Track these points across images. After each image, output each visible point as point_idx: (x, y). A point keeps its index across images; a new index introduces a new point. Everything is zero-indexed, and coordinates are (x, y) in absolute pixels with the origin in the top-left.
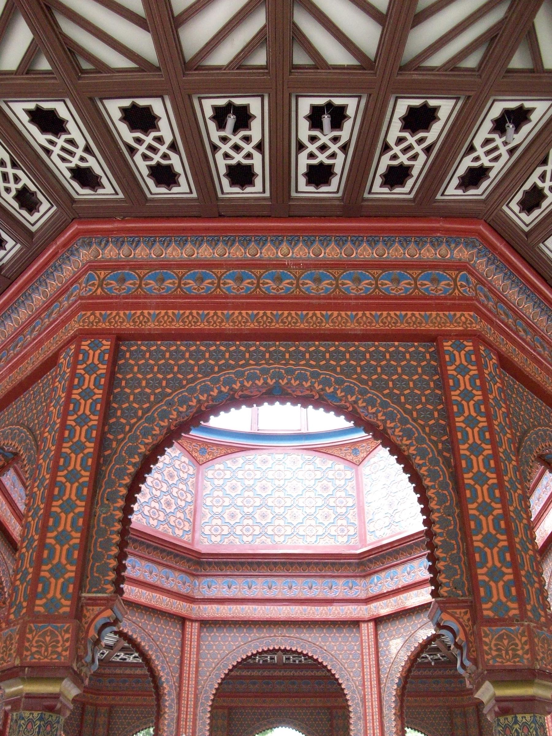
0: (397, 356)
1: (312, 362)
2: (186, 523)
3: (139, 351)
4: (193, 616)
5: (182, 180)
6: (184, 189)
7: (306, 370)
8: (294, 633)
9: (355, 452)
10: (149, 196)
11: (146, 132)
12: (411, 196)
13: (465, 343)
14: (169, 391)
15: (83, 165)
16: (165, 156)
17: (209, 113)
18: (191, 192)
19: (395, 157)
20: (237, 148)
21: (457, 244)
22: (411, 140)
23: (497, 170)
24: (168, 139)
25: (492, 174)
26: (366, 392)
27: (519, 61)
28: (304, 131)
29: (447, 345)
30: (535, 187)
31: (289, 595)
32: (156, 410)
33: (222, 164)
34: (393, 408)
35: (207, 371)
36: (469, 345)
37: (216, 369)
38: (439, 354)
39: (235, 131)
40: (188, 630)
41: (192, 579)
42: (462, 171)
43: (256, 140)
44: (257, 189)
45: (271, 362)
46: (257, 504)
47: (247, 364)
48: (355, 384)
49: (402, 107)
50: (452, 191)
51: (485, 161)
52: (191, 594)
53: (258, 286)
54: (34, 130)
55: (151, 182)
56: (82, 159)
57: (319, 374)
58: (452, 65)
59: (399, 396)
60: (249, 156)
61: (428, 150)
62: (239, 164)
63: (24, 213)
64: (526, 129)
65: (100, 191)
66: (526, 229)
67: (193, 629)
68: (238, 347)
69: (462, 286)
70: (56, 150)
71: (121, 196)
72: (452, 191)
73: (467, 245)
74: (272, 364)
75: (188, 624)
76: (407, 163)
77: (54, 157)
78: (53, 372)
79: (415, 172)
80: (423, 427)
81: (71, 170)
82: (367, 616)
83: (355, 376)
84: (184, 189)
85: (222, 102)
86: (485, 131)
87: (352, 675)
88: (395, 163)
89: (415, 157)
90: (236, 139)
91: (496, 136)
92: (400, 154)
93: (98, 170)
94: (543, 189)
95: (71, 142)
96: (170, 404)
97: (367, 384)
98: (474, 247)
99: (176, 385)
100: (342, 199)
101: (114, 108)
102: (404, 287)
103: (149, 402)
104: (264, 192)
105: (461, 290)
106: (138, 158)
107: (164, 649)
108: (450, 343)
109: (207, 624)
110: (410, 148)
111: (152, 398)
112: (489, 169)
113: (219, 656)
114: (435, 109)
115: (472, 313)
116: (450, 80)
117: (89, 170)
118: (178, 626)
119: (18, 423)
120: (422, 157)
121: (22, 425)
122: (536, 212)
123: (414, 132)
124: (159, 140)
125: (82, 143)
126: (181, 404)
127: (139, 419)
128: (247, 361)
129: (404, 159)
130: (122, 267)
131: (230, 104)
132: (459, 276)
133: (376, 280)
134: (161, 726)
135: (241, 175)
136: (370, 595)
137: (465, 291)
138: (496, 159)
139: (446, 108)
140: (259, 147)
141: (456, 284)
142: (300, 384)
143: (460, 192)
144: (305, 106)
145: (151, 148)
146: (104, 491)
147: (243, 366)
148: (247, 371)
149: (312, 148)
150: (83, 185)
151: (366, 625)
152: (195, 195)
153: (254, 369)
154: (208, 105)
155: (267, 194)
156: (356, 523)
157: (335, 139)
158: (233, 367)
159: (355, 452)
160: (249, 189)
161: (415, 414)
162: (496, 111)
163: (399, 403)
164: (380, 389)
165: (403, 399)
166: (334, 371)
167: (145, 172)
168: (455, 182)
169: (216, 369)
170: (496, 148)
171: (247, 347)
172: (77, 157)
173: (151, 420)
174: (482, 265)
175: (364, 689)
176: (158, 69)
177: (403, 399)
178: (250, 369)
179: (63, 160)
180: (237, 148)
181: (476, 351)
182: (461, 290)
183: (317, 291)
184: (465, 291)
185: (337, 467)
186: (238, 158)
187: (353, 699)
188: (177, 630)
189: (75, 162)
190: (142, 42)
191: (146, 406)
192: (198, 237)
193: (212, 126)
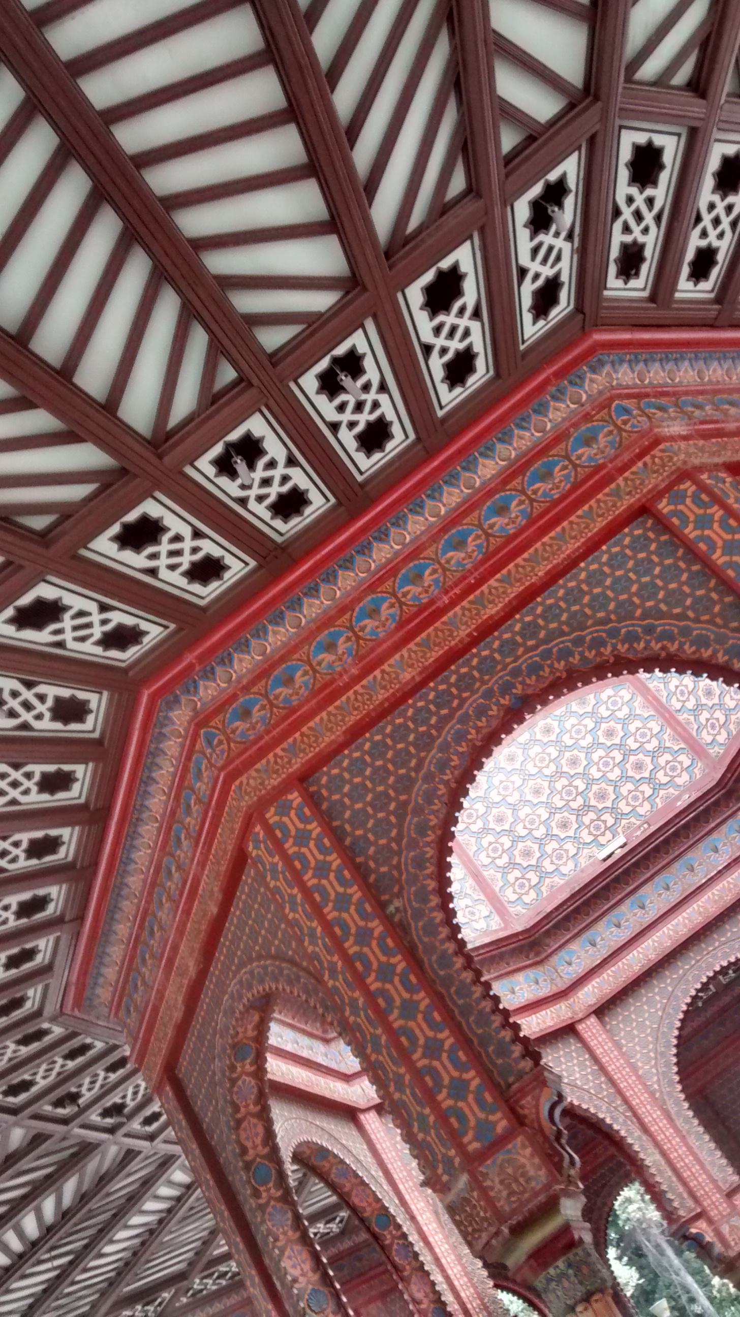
0: (615, 562)
1: (530, 643)
2: (479, 907)
3: (332, 779)
4: (580, 1016)
5: (229, 560)
6: (237, 567)
7: (531, 658)
10: (202, 603)
11: (155, 540)
12: (492, 372)
13: (682, 487)
14: (403, 797)
15: (108, 627)
16: (195, 550)
17: (211, 471)
18: (247, 564)
19: (444, 351)
20: (266, 482)
21: (582, 378)
22: (449, 319)
23: (566, 269)
24: (187, 532)
25: (564, 278)
26: (618, 630)
27: (509, 140)
28: (326, 408)
29: (664, 506)
30: (625, 247)
31: (674, 897)
32: (409, 829)
33: (262, 510)
34: (661, 625)
35: (425, 743)
36: (688, 487)
37: (434, 732)
38: (663, 525)
39: (251, 466)
40: (586, 1035)
41: (540, 968)
42: (527, 300)
43: (281, 458)
44: (319, 502)
45: (486, 677)
47: (463, 701)
48: (597, 631)
49: (415, 294)
50: (531, 329)
51: (547, 272)
52: (555, 990)
53: (401, 604)
54: (29, 634)
55: (197, 588)
56: (104, 622)
57: (549, 651)
58: (441, 208)
59: (656, 606)
60: (285, 479)
61: (476, 314)
62: (281, 497)
63: (74, 726)
64: (569, 202)
65: (146, 640)
66: (646, 294)
67: (591, 1029)
68: (435, 689)
69: (625, 422)
70: (68, 636)
71: (172, 626)
72: (531, 329)
73: (594, 370)
74: (489, 680)
75: (580, 1027)
76: (461, 346)
77: (71, 644)
78: (250, 873)
79: (478, 348)
80: (711, 622)
81: (99, 643)
83: (590, 622)
84: (237, 567)
85: (217, 450)
86: (524, 242)
88: (449, 356)
89: (467, 333)
90: (260, 473)
91: (541, 237)
92: (447, 343)
93: (129, 621)
94: (635, 242)
95: (81, 614)
96: (418, 810)
97: (611, 621)
98: (602, 363)
99: (406, 784)
100: (418, 439)
101: (104, 546)
102: (561, 477)
103: (393, 826)
104: (328, 500)
105: (628, 427)
106: (164, 574)
107: (579, 1082)
108: (665, 501)
109: (602, 1011)
110: (454, 329)
111: (393, 819)
112: (557, 275)
114: (455, 268)
115: (661, 447)
116: (447, 220)
117: (120, 628)
119: (251, 960)
120: (475, 326)
121: (260, 957)
122: (644, 268)
123: (447, 308)
124: (178, 538)
125: (92, 607)
126: (430, 802)
127: (399, 853)
128: (459, 697)
129: (456, 345)
130: (233, 698)
131: (228, 445)
132: (613, 414)
133: (523, 492)
134: (651, 1181)
135: (290, 504)
137: (633, 426)
138: (558, 258)
139: (464, 257)
140: (291, 461)
141: (616, 425)
142: (539, 678)
143: (541, 323)
144: (310, 381)
145: (172, 554)
146: (431, 960)
147: (460, 706)
148: (469, 707)
149: (347, 416)
150: (123, 647)
152: (253, 563)
153: (474, 701)
154: (205, 464)
155: (333, 500)
157: (366, 388)
158: (450, 716)
160: (308, 511)
161: (691, 614)
162: (522, 210)
163: (661, 615)
164: (630, 616)
165: (663, 607)
166: (563, 634)
167: (183, 582)
168: (528, 317)
169: (434, 732)
170: (551, 249)
171: (446, 681)
172: (96, 623)
173: (413, 844)
174: (625, 375)
176: (123, 472)
177: (663, 607)
178: (471, 705)
179: (83, 639)
180: (266, 482)
181: (702, 488)
182: (628, 427)
183: (470, 557)
184: (633, 426)
185: (604, 696)
186: (274, 491)
188: (573, 1045)
189: (97, 632)
190: (85, 456)
191: (394, 833)
192: (290, 600)
193: (224, 481)
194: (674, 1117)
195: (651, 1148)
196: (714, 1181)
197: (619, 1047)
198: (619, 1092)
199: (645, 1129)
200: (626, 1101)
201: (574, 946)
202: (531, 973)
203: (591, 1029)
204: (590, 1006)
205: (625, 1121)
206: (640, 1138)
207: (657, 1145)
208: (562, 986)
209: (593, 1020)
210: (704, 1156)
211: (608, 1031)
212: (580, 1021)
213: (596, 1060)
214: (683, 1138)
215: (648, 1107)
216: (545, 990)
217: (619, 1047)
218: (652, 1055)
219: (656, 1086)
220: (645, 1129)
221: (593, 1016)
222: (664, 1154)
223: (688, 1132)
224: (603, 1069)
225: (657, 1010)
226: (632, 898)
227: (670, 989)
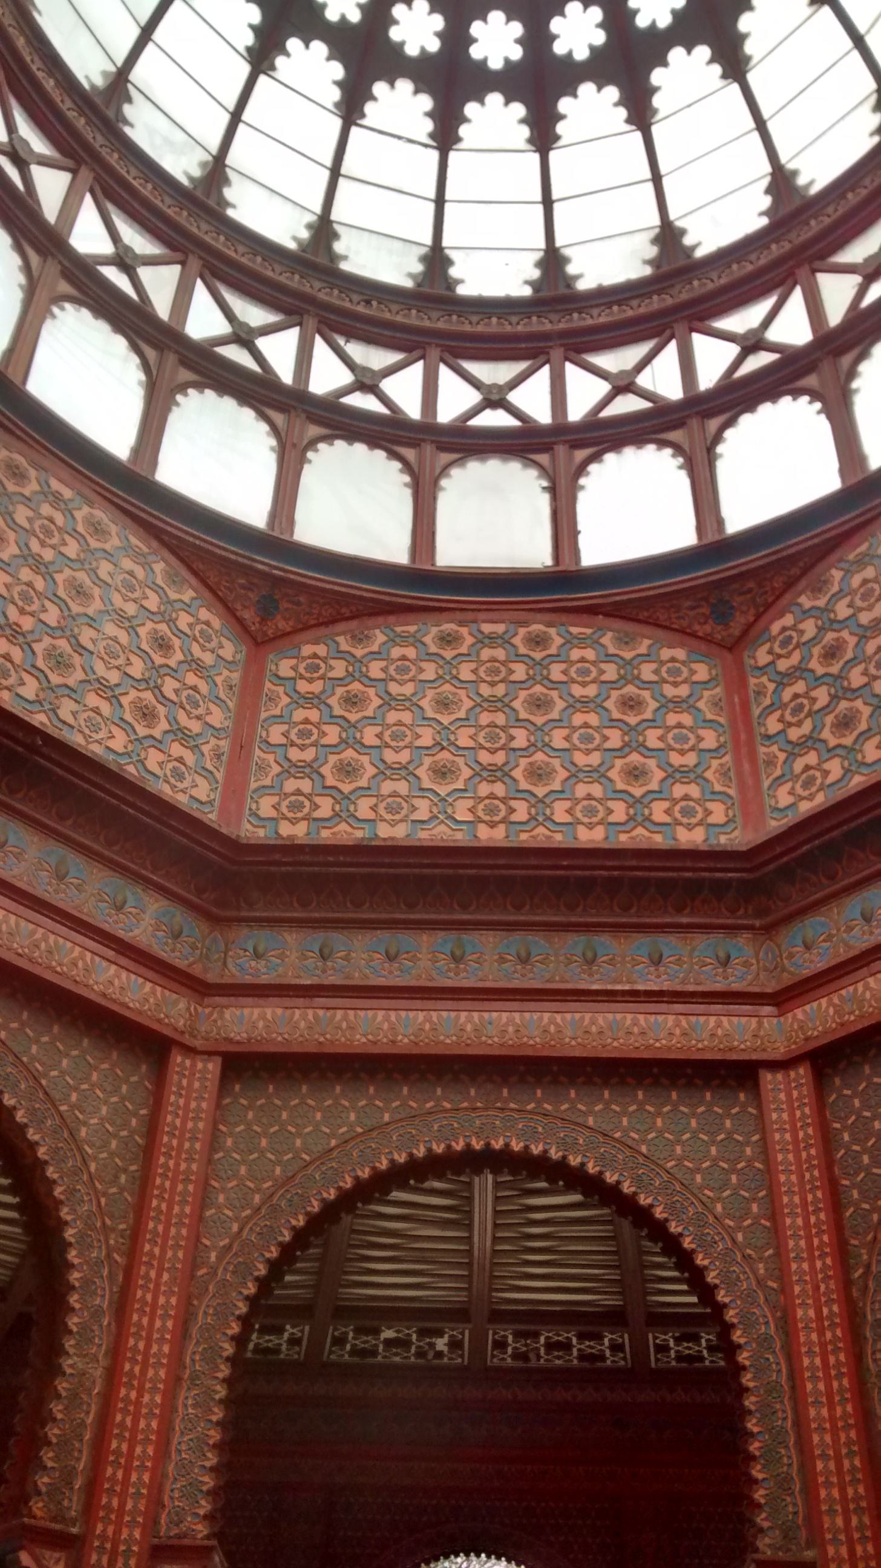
8: (538, 1100)
9: (722, 614)
41: (205, 927)
46: (426, 740)
52: (197, 971)
75: (178, 1059)
82: (779, 1050)
87: (740, 1237)
107: (83, 1132)
113: (278, 1170)
118: (144, 1067)
136: (787, 980)
151: (779, 1076)
156: (732, 792)
159: (722, 614)
175: (785, 1289)
185: (666, 653)
187: (748, 1323)
194: (194, 1331)
195: (100, 1346)
196: (156, 1502)
197: (214, 1142)
198: (140, 1209)
199: (122, 1307)
200: (135, 1235)
201: (291, 937)
202: (179, 916)
203: (194, 1080)
204: (230, 1041)
205: (99, 1263)
206: (97, 1313)
207: (116, 1353)
208: (211, 978)
209: (213, 1067)
210: (181, 1442)
211: (218, 1106)
212: (190, 1051)
213: (152, 1128)
214: (175, 1381)
215: (166, 1276)
216: (179, 957)
217: (214, 1142)
218: (257, 1198)
219: (213, 1256)
220: (122, 1307)
221: (219, 1060)
222: (112, 1375)
223: (194, 1377)
224: (149, 1152)
225: (333, 1135)
226: (453, 935)
227: (387, 1117)
